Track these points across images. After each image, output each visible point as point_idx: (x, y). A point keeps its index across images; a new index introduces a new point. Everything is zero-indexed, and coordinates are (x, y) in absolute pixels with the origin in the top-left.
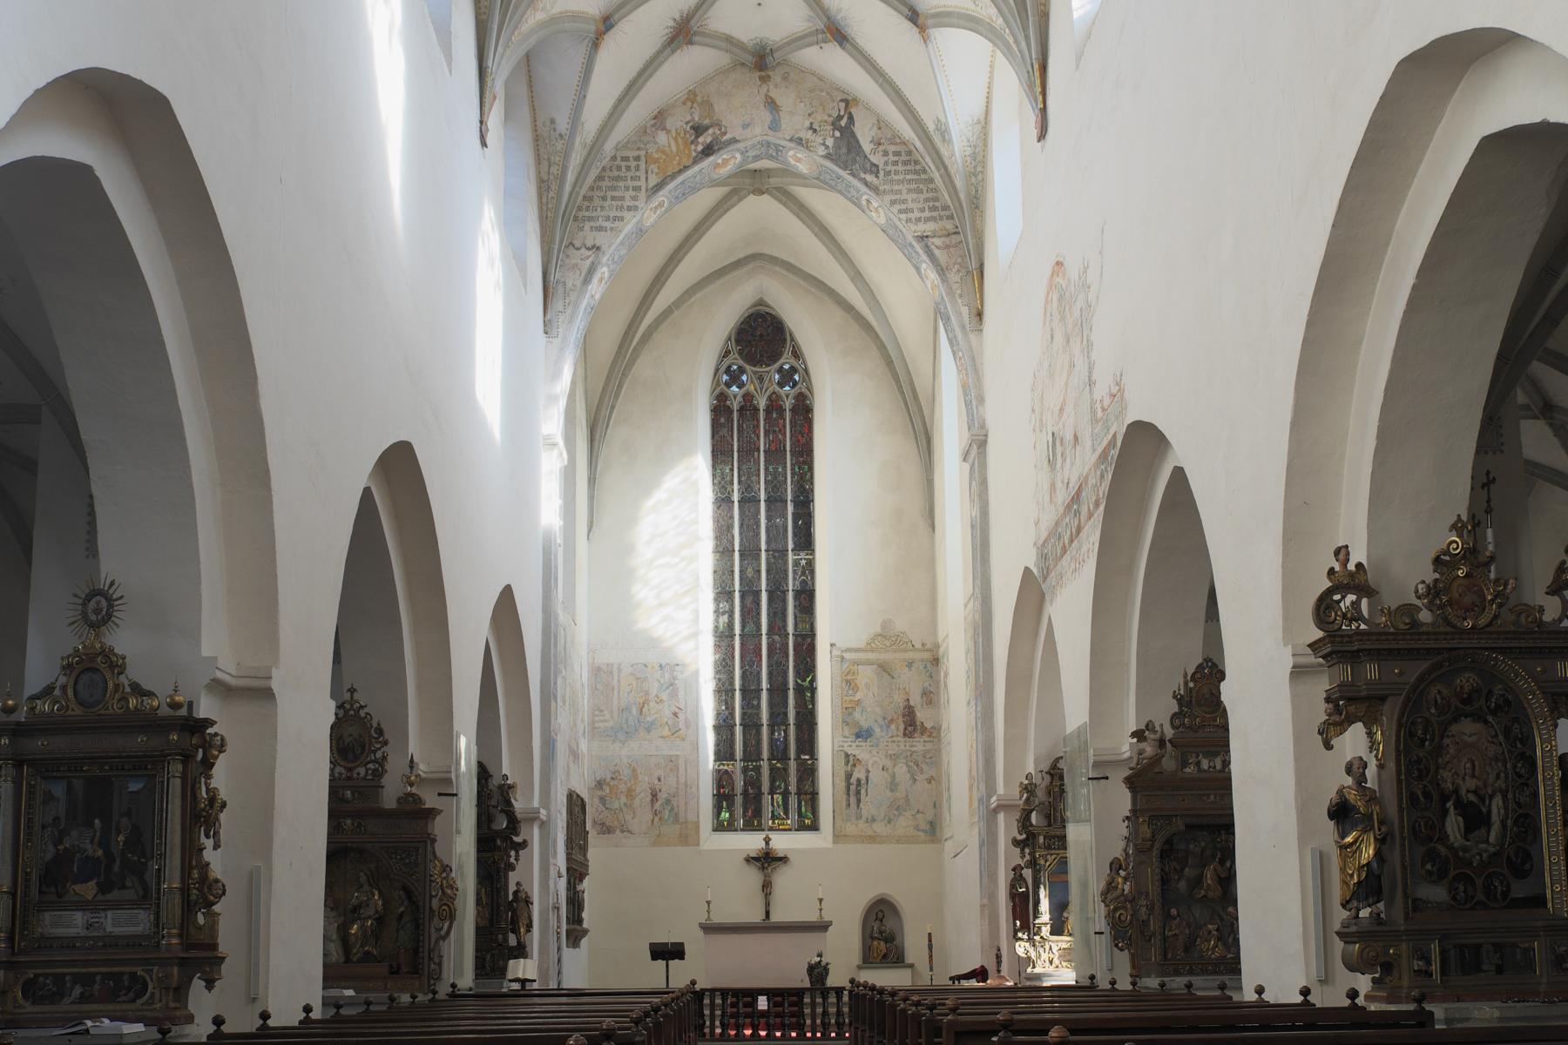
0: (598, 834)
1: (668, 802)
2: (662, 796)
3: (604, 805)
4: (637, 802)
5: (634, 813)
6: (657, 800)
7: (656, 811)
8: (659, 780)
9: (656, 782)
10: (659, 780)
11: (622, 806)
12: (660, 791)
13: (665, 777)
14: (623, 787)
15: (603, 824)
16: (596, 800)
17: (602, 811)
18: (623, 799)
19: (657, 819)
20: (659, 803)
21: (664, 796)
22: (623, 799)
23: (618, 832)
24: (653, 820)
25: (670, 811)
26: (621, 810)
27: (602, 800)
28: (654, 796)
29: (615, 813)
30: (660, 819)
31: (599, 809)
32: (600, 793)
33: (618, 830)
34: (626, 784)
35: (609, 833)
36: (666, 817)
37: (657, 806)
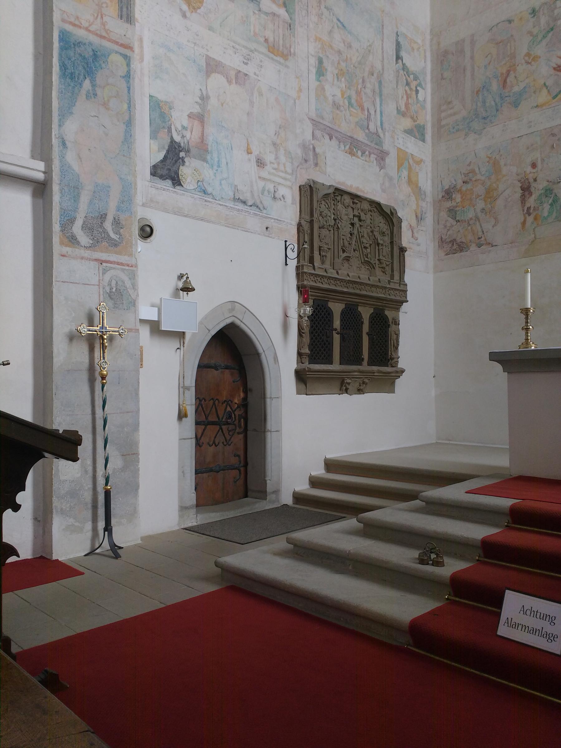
0: (447, 255)
1: (548, 192)
2: (539, 187)
3: (454, 218)
4: (500, 203)
5: (496, 219)
6: (531, 194)
7: (529, 208)
8: (534, 165)
9: (529, 169)
10: (534, 165)
11: (479, 214)
12: (535, 180)
13: (543, 160)
14: (480, 190)
15: (453, 241)
16: (444, 215)
17: (452, 226)
18: (480, 204)
19: (530, 219)
20: (533, 197)
21: (541, 187)
22: (480, 204)
23: (473, 247)
24: (524, 223)
25: (551, 205)
26: (477, 218)
27: (452, 212)
28: (526, 190)
29: (470, 225)
30: (535, 219)
31: (448, 224)
32: (449, 204)
33: (474, 245)
34: (483, 184)
35: (461, 251)
36: (546, 214)
37: (531, 202)
